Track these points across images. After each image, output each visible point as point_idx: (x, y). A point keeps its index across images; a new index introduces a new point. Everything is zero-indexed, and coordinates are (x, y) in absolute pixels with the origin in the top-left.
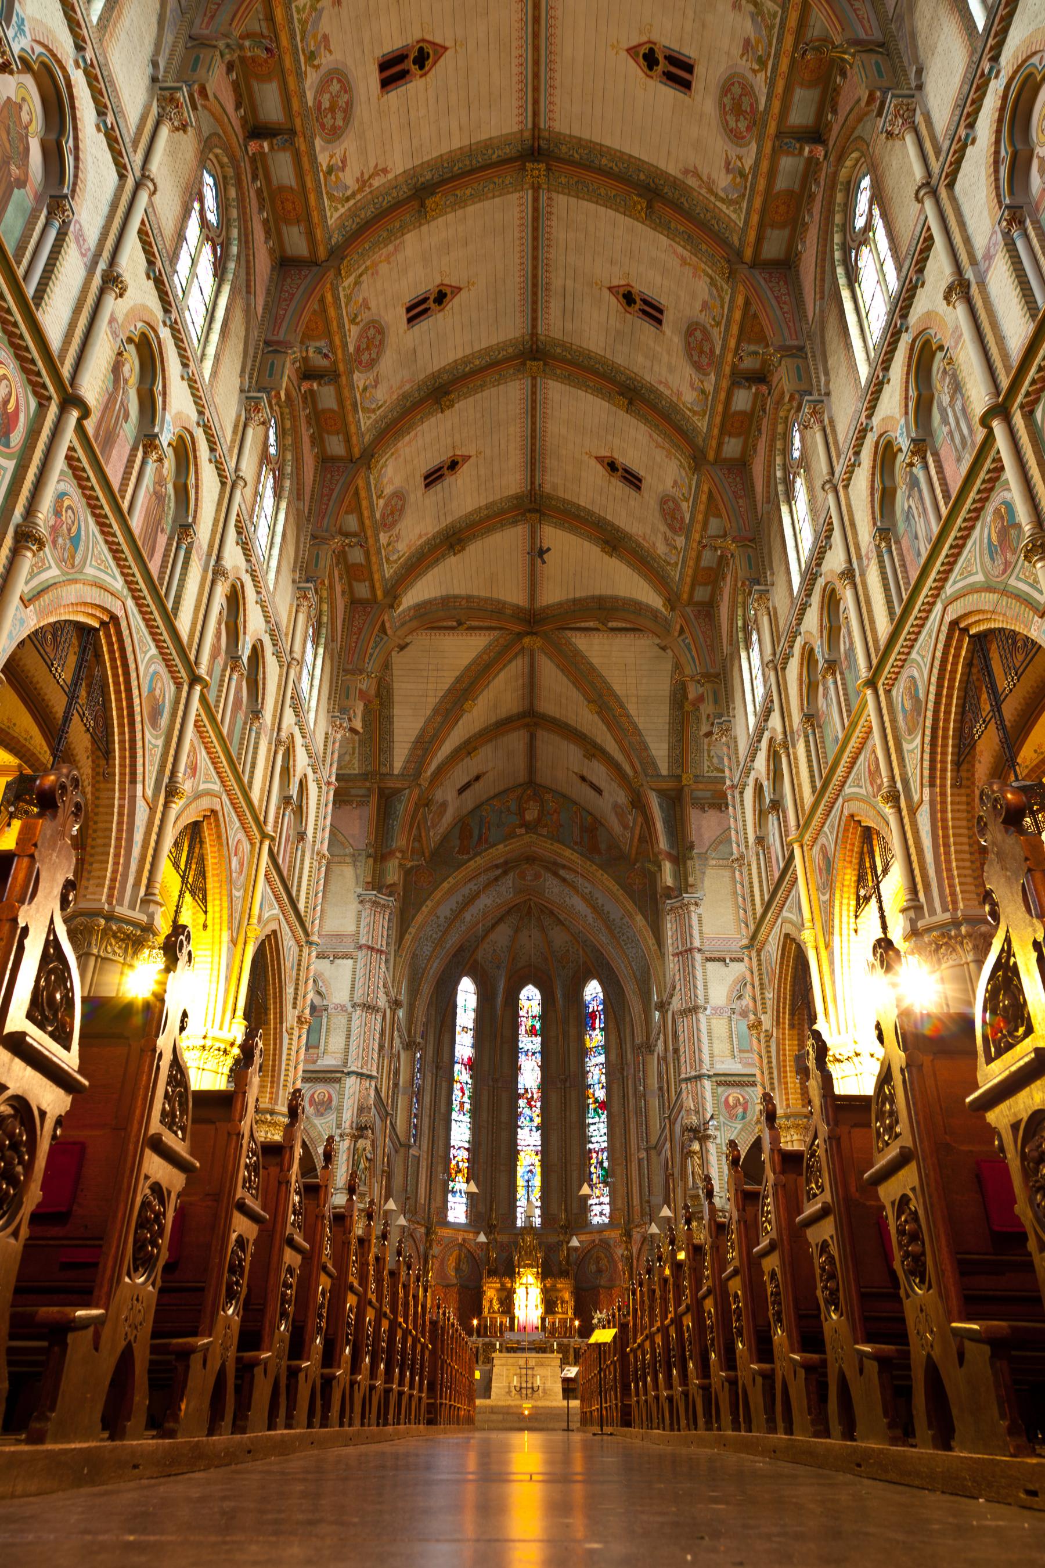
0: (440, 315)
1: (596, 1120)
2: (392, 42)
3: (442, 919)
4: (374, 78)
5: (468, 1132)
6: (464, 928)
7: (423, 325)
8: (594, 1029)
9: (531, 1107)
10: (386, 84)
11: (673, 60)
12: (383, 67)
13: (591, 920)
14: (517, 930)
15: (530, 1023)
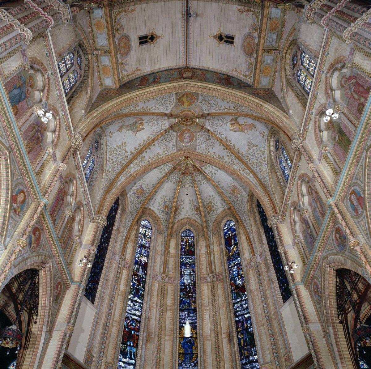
0: (152, 45)
1: (238, 300)
2: (144, 33)
3: (129, 153)
4: (137, 41)
5: (140, 309)
6: (144, 164)
7: (144, 47)
8: (231, 246)
9: (189, 297)
10: (141, 43)
11: (227, 37)
12: (140, 38)
13: (226, 159)
14: (180, 182)
15: (188, 248)
